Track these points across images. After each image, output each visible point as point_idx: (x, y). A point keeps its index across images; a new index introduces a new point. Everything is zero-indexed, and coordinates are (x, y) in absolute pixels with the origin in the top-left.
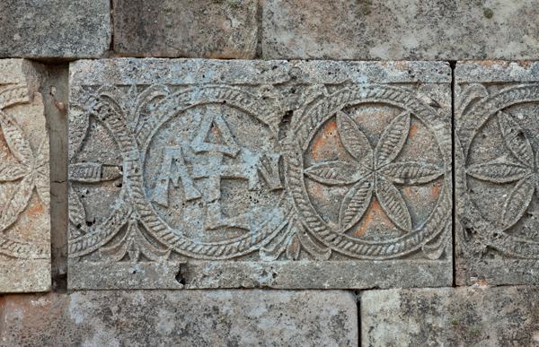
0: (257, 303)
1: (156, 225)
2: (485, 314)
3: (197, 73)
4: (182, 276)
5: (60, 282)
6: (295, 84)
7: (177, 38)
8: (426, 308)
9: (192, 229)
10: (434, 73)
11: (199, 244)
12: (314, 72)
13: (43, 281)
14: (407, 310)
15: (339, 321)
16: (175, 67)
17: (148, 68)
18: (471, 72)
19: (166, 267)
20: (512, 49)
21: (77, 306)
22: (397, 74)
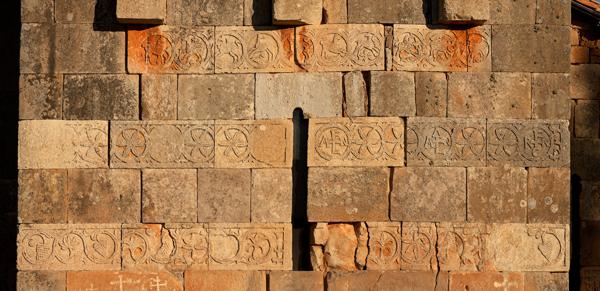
0: (445, 169)
1: (426, 152)
2: (492, 172)
3: (434, 120)
4: (431, 163)
5: (406, 164)
6: (455, 123)
7: (430, 113)
8: (480, 171)
9: (431, 153)
10: (483, 121)
11: (433, 157)
12: (457, 120)
13: (403, 164)
14: (476, 171)
15: (462, 173)
16: (429, 119)
17: (424, 119)
18: (491, 121)
19: (428, 161)
20: (499, 116)
21: (409, 170)
22: (475, 121)
